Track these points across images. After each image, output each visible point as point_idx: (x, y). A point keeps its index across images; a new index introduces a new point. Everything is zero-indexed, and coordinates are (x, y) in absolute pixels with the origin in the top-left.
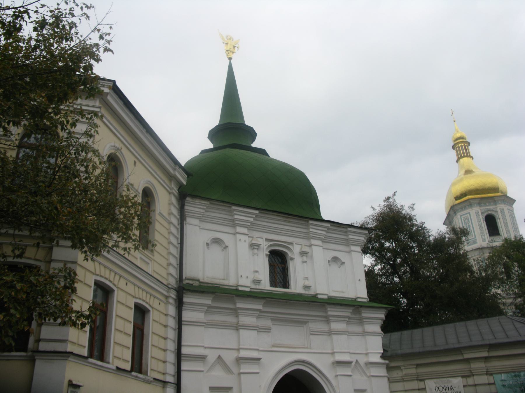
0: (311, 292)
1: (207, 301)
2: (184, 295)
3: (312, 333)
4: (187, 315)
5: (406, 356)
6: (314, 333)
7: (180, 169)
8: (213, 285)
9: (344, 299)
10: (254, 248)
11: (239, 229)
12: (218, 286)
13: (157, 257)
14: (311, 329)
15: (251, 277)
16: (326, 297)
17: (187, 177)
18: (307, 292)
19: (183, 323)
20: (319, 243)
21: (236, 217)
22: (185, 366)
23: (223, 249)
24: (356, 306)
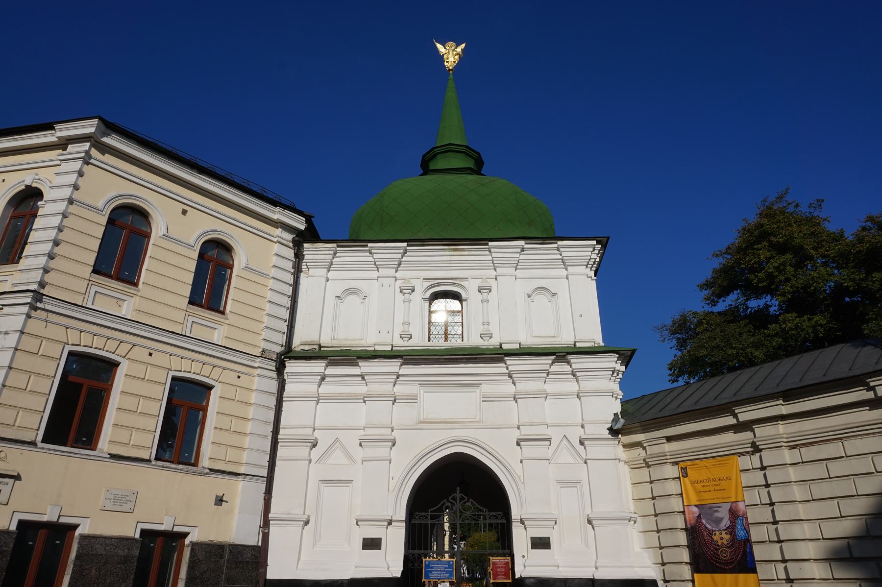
0: (494, 342)
1: (318, 366)
2: (287, 364)
3: (484, 399)
4: (290, 388)
5: (646, 427)
6: (486, 399)
7: (285, 210)
8: (342, 348)
9: (553, 346)
10: (404, 294)
11: (383, 272)
12: (349, 348)
13: (231, 318)
14: (483, 394)
15: (398, 330)
16: (517, 346)
17: (305, 220)
18: (486, 343)
19: (284, 399)
20: (511, 270)
21: (375, 256)
22: (281, 452)
23: (363, 301)
24: (557, 354)
